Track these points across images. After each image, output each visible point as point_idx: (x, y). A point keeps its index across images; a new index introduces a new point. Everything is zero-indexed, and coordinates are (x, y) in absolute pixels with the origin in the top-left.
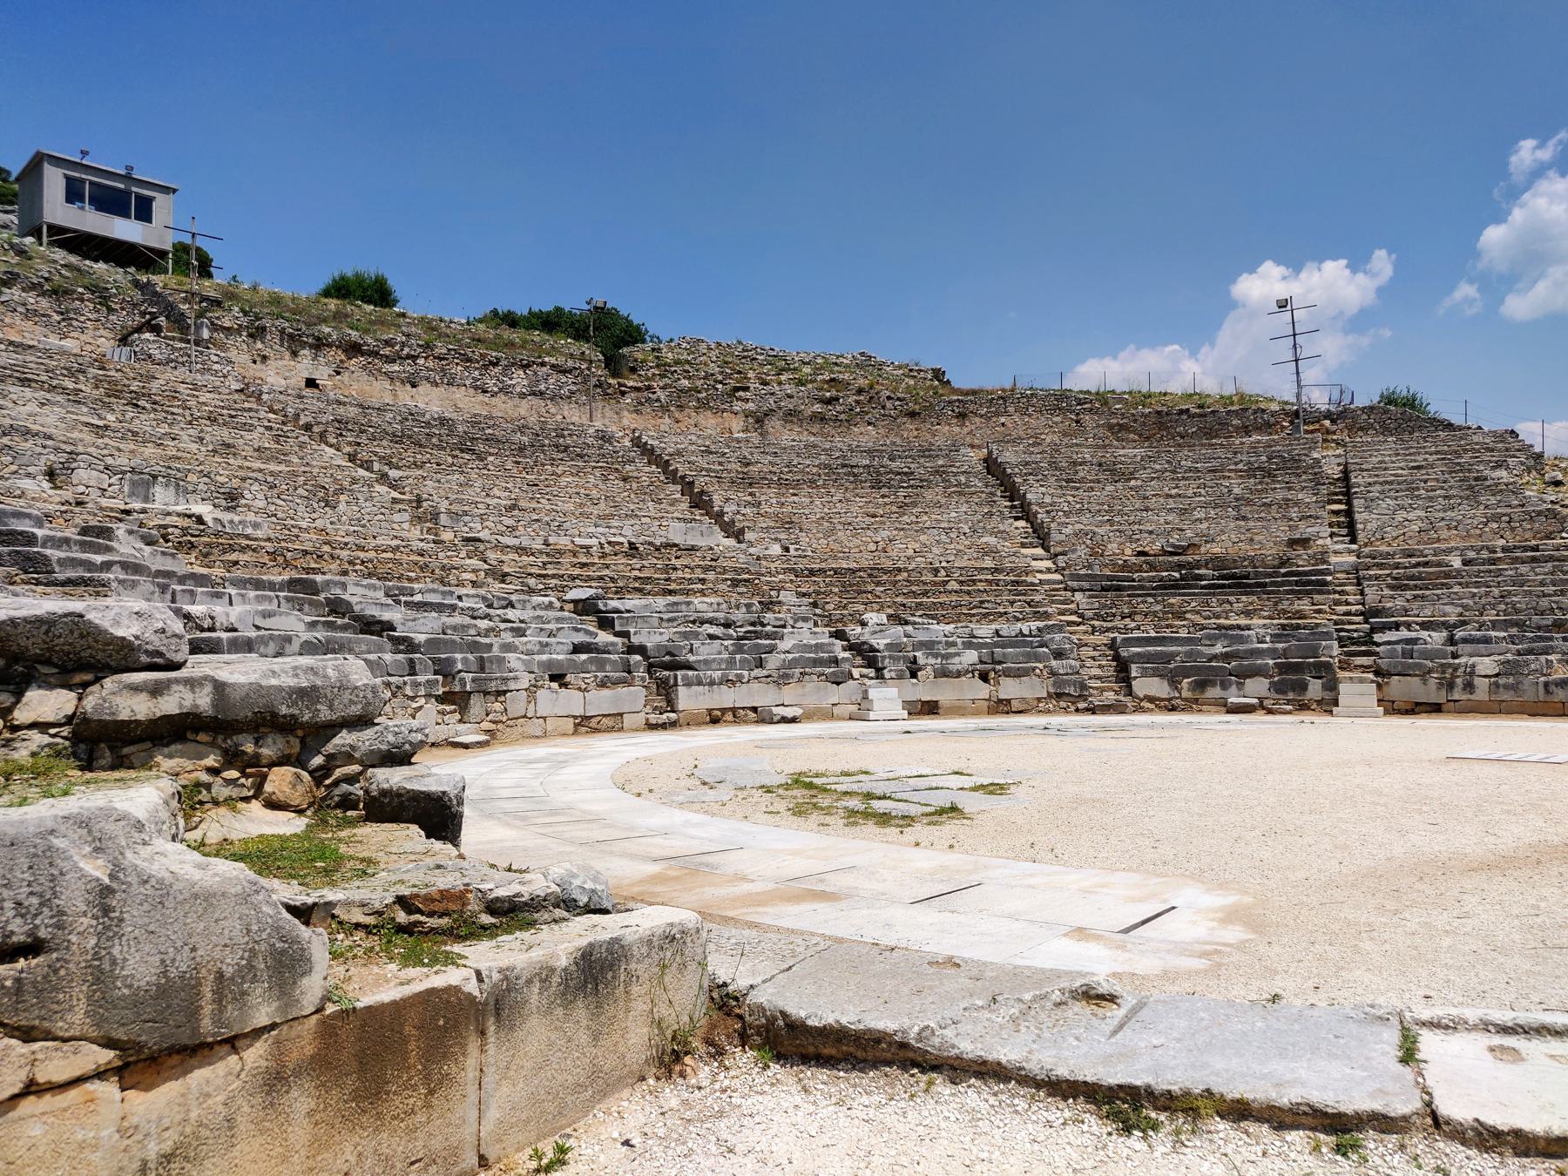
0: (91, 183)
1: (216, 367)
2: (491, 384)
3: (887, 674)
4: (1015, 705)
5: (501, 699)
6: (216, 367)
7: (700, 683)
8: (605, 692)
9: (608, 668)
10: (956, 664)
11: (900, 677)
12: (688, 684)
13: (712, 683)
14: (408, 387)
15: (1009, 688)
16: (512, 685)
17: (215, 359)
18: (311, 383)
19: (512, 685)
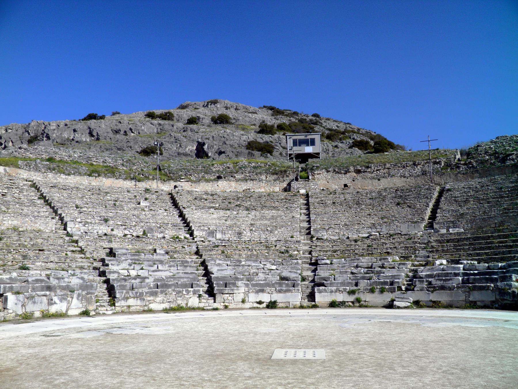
0: (300, 140)
1: (313, 187)
2: (407, 174)
3: (415, 289)
4: (479, 303)
5: (231, 295)
6: (313, 187)
7: (325, 291)
8: (281, 295)
9: (284, 286)
10: (449, 284)
11: (422, 290)
12: (320, 292)
13: (332, 292)
14: (377, 181)
15: (475, 296)
16: (235, 291)
17: (312, 184)
18: (346, 186)
19: (235, 291)
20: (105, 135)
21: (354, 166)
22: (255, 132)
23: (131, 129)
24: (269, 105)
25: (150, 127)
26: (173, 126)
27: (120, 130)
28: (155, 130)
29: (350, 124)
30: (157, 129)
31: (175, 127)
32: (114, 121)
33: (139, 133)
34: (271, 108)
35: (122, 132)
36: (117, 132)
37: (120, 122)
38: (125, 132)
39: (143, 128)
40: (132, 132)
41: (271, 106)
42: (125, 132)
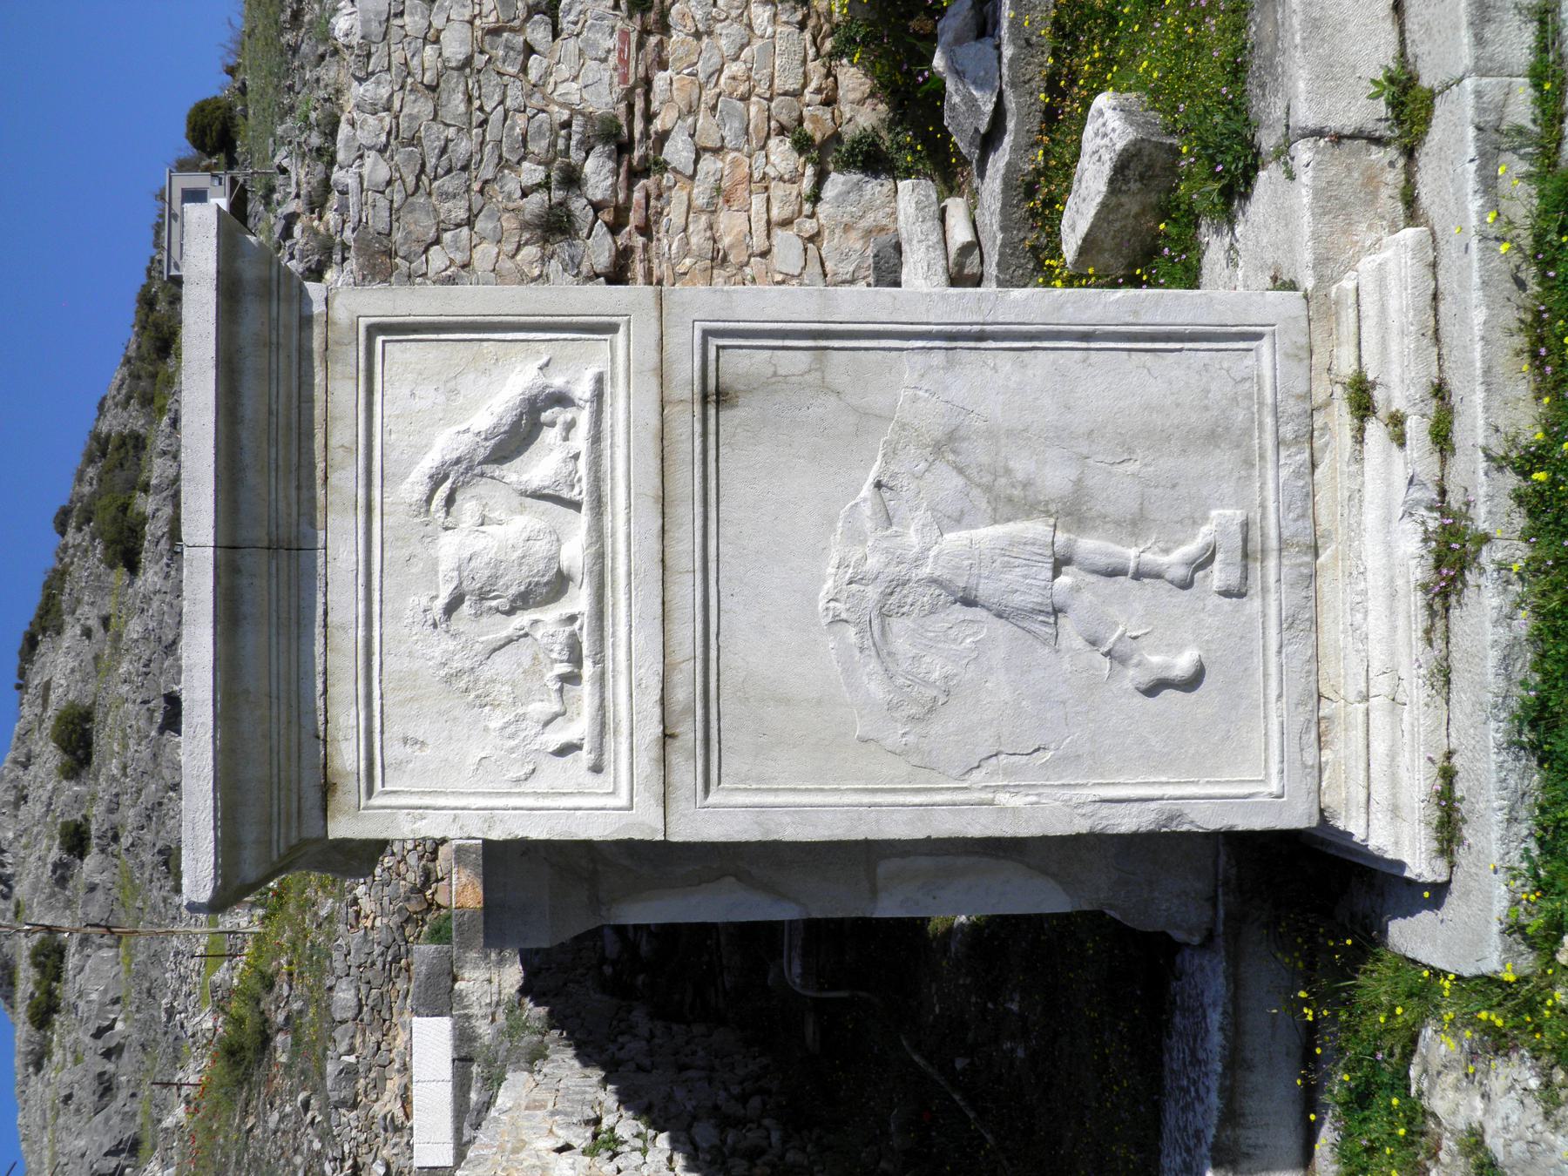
20: (116, 1119)
21: (280, 34)
22: (131, 584)
23: (99, 1034)
24: (16, 660)
25: (92, 970)
26: (92, 888)
27: (101, 1074)
28: (107, 953)
29: (104, 399)
30: (100, 947)
31: (97, 879)
32: (61, 1121)
33: (116, 1001)
34: (31, 643)
35: (110, 1067)
36: (106, 1087)
37: (69, 1097)
38: (108, 1054)
39: (94, 996)
40: (111, 1027)
41: (21, 653)
42: (108, 1054)
